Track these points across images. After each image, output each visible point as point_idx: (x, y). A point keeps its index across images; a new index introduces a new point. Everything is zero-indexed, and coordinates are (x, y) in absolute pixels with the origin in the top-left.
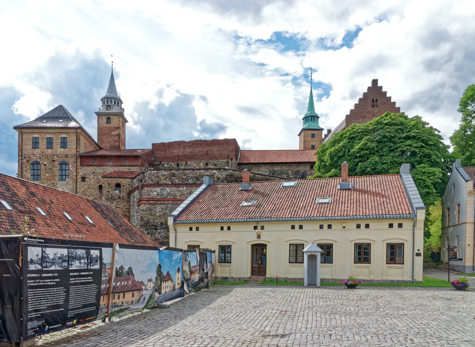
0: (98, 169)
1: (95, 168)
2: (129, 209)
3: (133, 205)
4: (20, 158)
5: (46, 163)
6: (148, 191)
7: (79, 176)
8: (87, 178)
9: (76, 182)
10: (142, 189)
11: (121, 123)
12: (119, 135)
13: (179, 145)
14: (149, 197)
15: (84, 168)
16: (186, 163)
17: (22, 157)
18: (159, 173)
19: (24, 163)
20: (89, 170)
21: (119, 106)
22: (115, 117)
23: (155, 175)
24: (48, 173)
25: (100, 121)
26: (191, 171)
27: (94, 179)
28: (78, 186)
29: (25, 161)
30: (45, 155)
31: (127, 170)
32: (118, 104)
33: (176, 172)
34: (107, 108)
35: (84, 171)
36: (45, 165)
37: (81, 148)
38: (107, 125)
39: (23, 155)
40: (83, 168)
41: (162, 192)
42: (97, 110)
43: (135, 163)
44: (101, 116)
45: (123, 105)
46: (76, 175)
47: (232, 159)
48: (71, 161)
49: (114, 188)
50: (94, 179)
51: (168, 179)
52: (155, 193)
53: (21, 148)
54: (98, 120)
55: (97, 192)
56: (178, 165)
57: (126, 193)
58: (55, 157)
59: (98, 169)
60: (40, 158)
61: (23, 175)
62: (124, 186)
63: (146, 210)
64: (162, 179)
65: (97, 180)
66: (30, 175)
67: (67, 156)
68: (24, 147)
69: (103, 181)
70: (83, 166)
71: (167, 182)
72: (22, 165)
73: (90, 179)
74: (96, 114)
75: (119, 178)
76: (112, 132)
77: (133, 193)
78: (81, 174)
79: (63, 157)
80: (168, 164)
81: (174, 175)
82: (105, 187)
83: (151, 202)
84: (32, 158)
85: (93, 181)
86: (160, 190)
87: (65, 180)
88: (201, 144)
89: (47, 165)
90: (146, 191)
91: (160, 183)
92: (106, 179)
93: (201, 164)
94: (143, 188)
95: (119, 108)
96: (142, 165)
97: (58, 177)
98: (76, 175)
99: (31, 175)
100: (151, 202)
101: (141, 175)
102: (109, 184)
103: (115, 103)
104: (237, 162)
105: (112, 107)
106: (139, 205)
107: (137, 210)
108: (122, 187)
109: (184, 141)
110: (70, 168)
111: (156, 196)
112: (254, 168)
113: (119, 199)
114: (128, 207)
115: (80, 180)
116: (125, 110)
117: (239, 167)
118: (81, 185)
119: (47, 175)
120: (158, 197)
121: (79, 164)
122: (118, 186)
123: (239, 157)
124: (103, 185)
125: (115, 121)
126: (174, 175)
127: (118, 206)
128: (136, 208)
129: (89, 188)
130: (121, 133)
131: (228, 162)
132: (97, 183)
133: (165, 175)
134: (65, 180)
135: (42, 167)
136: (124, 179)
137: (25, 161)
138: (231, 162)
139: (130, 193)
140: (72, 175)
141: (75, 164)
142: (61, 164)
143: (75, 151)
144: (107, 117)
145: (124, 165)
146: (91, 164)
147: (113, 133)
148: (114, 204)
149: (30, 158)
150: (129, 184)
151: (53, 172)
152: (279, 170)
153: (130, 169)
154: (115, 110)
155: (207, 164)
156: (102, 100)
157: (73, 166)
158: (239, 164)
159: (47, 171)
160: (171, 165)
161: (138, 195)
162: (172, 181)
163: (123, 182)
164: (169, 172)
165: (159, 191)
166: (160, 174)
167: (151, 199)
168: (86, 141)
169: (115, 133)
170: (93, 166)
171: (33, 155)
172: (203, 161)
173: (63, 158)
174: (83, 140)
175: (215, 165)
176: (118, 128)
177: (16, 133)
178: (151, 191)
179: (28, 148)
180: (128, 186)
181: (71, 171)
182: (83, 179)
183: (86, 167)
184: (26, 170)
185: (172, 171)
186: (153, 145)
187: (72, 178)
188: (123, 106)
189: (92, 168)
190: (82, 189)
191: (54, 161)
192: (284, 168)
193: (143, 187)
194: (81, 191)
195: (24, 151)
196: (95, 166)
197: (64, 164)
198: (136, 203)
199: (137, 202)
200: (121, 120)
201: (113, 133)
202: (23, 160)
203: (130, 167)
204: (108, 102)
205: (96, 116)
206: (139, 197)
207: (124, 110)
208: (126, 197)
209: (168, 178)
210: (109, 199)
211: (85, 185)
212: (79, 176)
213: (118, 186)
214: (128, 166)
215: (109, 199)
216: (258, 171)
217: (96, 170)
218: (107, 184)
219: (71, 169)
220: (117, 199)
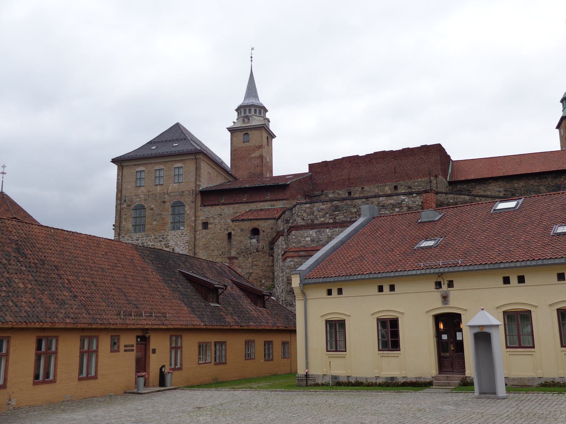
1: (222, 207)
2: (273, 266)
3: (278, 260)
4: (119, 202)
5: (153, 206)
6: (298, 236)
9: (195, 231)
10: (288, 234)
11: (265, 140)
12: (261, 157)
13: (350, 162)
14: (299, 246)
15: (206, 209)
16: (363, 188)
17: (121, 200)
18: (314, 206)
19: (123, 209)
21: (262, 115)
22: (255, 131)
23: (308, 210)
24: (155, 220)
25: (234, 139)
26: (364, 200)
27: (221, 225)
28: (198, 237)
29: (125, 206)
30: (153, 194)
31: (269, 207)
32: (260, 113)
33: (340, 204)
34: (244, 120)
36: (152, 209)
37: (202, 180)
38: (244, 145)
39: (123, 197)
40: (205, 210)
41: (318, 237)
42: (231, 125)
43: (280, 196)
44: (235, 132)
45: (267, 114)
46: (195, 220)
47: (436, 176)
48: (188, 200)
49: (249, 235)
50: (221, 225)
51: (328, 215)
52: (308, 239)
53: (120, 188)
54: (231, 139)
55: (226, 243)
56: (350, 193)
57: (268, 242)
58: (166, 196)
60: (146, 200)
61: (122, 225)
62: (263, 231)
63: (295, 266)
64: (318, 217)
65: (225, 225)
66: (131, 225)
67: (182, 193)
68: (124, 186)
69: (233, 227)
70: (204, 206)
71: (327, 221)
72: (121, 212)
73: (215, 225)
74: (229, 131)
75: (257, 219)
76: (251, 154)
77: (276, 241)
79: (176, 196)
80: (334, 192)
81: (337, 208)
82: (235, 235)
83: (302, 253)
84: (135, 201)
85: (219, 227)
86: (316, 233)
88: (384, 158)
89: (155, 209)
90: (294, 237)
91: (316, 222)
92: (237, 223)
93: (387, 188)
94: (291, 232)
95: (262, 119)
96: (293, 197)
97: (169, 226)
98: (195, 220)
99: (133, 225)
100: (302, 253)
101: (287, 213)
102: (242, 230)
103: (255, 112)
104: (447, 180)
105: (251, 118)
106: (284, 260)
107: (283, 268)
108: (261, 233)
109: (357, 156)
110: (186, 211)
111: (310, 243)
112: (478, 187)
113: (257, 251)
114: (271, 264)
115: (200, 227)
116: (270, 120)
117: (450, 187)
118: (201, 233)
119: (155, 223)
120: (313, 245)
121: (199, 203)
122: (255, 232)
123: (450, 171)
124: (233, 233)
125: (255, 138)
126: (337, 208)
127: (256, 263)
128: (281, 264)
129: (213, 239)
130: (264, 154)
131: (431, 182)
132: (225, 229)
133: (323, 210)
135: (148, 212)
136: (263, 221)
137: (125, 206)
138: (435, 182)
139: (273, 243)
141: (194, 204)
142: (173, 206)
143: (194, 185)
144: (243, 133)
145: (265, 199)
146: (217, 203)
147: (253, 155)
148: (250, 260)
149: (132, 201)
150: (272, 228)
151: (163, 219)
152: (523, 187)
153: (274, 206)
154: (256, 121)
155: (396, 188)
156: (237, 110)
157: (191, 208)
158: (450, 183)
159: (155, 218)
160: (339, 194)
161: (283, 243)
162: (335, 218)
163: (263, 225)
164: (329, 205)
165: (314, 235)
166: (315, 209)
167: (302, 249)
168: (210, 170)
169: (257, 154)
170: (218, 205)
171: (136, 197)
172: (388, 184)
173: (176, 197)
174: (205, 168)
175: (410, 188)
176: (261, 147)
177: (115, 167)
178: (302, 236)
179: (129, 187)
180: (270, 231)
181: (188, 214)
182: (205, 225)
183: (209, 207)
184: (126, 219)
185: (334, 203)
186: (311, 166)
188: (268, 115)
189: (218, 207)
190: (204, 240)
191: (164, 202)
192: (531, 182)
193: (290, 230)
194: (202, 244)
195: (124, 193)
196: (223, 204)
197: (178, 205)
198: (280, 257)
199: (283, 255)
200: (265, 135)
201: (253, 155)
202: (123, 204)
203: (273, 203)
204: (245, 112)
205: (229, 134)
206: (284, 247)
207: (269, 121)
208: (267, 249)
209: (328, 213)
210: (242, 253)
211: (207, 234)
212: (199, 222)
213: (255, 232)
214: (270, 201)
215: (242, 253)
216: (485, 191)
217: (224, 210)
218: (239, 230)
219: (188, 212)
220: (254, 253)
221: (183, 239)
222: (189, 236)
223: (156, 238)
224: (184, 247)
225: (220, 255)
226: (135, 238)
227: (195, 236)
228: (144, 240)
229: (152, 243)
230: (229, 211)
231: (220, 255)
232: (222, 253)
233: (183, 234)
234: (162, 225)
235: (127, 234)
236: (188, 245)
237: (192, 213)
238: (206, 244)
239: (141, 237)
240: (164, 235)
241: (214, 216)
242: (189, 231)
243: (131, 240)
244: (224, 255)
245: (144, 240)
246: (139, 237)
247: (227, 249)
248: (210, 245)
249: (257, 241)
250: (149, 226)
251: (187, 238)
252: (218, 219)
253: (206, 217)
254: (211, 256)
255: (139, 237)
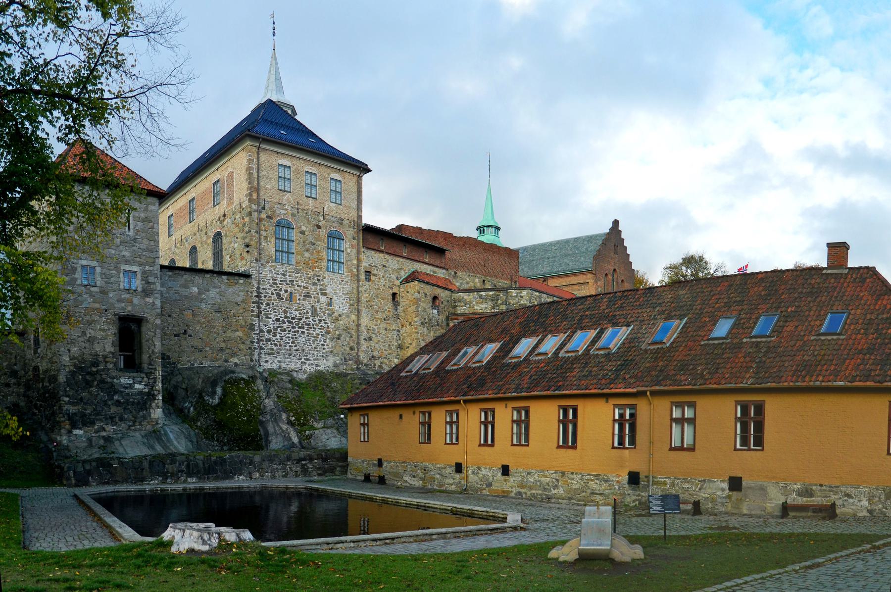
0: (390, 261)
1: (387, 256)
7: (362, 269)
8: (374, 275)
9: (358, 281)
15: (371, 253)
20: (377, 259)
28: (360, 289)
35: (372, 259)
50: (385, 280)
55: (390, 305)
57: (445, 317)
59: (390, 261)
65: (390, 281)
73: (379, 278)
75: (439, 287)
78: (364, 265)
85: (382, 282)
87: (338, 273)
99: (276, 251)
115: (363, 277)
118: (365, 286)
119: (307, 255)
134: (338, 273)
140: (349, 263)
181: (348, 254)
183: (373, 252)
187: (350, 271)
189: (381, 255)
190: (367, 295)
194: (365, 299)
212: (362, 269)
217: (388, 261)
221: (343, 288)
222: (350, 285)
223: (310, 278)
224: (344, 299)
225: (384, 319)
226: (281, 271)
227: (358, 287)
228: (293, 277)
229: (305, 285)
230: (393, 262)
231: (384, 319)
232: (387, 317)
233: (342, 281)
234: (316, 260)
235: (269, 262)
236: (349, 298)
237: (352, 254)
238: (369, 301)
239: (290, 272)
240: (320, 276)
241: (378, 266)
242: (349, 278)
243: (275, 273)
244: (388, 320)
245: (293, 277)
246: (286, 271)
247: (392, 313)
248: (373, 303)
249: (438, 312)
250: (299, 257)
251: (347, 288)
252: (383, 271)
253: (369, 265)
254: (375, 318)
255: (286, 271)
